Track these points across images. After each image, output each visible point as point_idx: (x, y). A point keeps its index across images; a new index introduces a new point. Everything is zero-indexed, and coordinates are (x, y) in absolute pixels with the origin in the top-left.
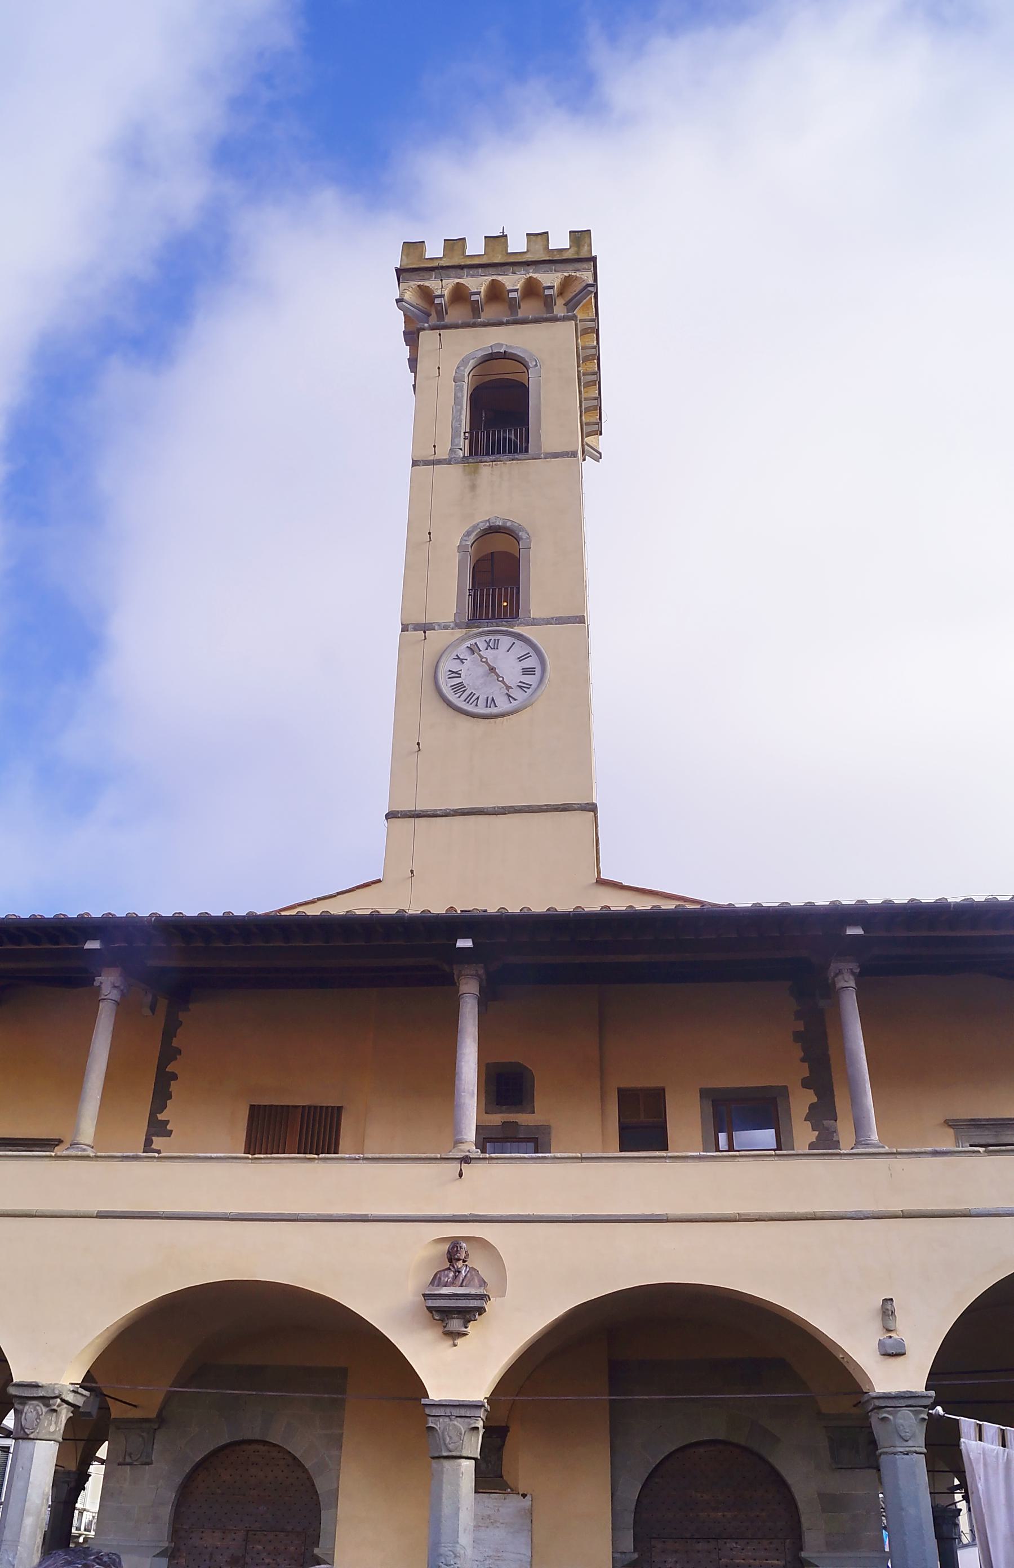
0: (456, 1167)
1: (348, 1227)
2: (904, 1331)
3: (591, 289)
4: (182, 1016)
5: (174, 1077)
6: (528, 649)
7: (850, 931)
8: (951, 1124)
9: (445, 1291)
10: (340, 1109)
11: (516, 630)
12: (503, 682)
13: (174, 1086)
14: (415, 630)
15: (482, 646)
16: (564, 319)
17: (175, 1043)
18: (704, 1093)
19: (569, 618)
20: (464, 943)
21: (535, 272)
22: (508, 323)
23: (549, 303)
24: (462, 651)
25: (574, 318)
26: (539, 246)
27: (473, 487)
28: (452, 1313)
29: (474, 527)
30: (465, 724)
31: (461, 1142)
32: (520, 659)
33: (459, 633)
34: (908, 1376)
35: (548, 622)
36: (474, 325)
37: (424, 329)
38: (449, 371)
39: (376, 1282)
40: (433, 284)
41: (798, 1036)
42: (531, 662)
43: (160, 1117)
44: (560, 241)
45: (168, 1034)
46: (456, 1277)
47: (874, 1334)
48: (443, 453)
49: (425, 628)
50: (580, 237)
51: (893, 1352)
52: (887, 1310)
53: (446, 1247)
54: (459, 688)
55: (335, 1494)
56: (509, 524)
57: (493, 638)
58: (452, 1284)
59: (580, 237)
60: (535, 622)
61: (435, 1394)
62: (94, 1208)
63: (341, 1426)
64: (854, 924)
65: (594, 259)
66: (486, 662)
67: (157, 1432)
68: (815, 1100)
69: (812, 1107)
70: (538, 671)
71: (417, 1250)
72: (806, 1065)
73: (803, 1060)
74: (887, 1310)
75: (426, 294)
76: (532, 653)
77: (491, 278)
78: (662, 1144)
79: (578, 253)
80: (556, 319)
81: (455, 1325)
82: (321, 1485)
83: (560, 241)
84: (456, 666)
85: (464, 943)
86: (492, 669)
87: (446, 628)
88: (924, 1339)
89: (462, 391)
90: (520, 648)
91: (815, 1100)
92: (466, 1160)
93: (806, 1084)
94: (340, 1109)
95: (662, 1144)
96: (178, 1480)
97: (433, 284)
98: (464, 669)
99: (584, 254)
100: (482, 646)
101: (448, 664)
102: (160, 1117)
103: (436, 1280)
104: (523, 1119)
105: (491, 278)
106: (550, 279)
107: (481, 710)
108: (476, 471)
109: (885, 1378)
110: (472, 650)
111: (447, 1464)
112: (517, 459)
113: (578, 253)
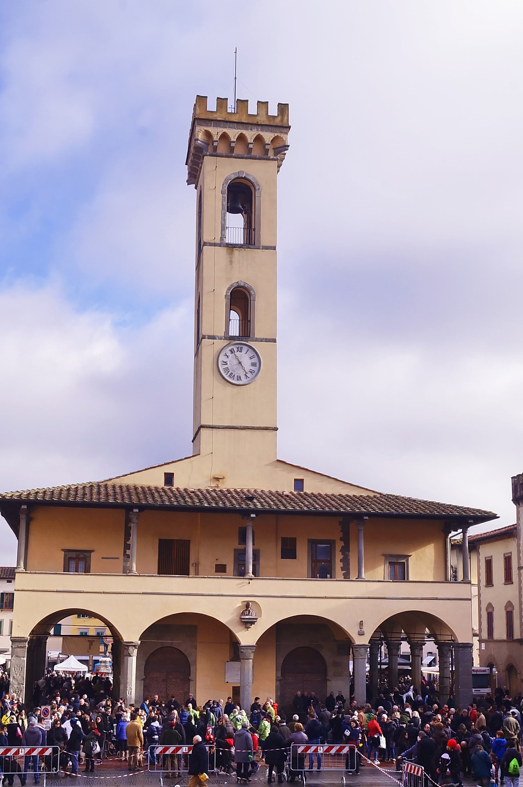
0: (247, 581)
2: (365, 629)
6: (254, 354)
8: (384, 555)
9: (247, 617)
11: (250, 343)
12: (244, 369)
14: (208, 338)
15: (235, 350)
16: (273, 159)
19: (270, 339)
20: (253, 516)
21: (262, 131)
22: (246, 158)
24: (227, 351)
26: (263, 113)
27: (231, 262)
28: (247, 623)
29: (232, 285)
30: (229, 388)
31: (249, 573)
32: (251, 358)
33: (226, 342)
34: (365, 640)
35: (262, 340)
37: (206, 155)
38: (220, 188)
41: (340, 523)
42: (255, 360)
43: (128, 543)
46: (249, 613)
48: (218, 241)
51: (361, 634)
52: (361, 623)
53: (246, 603)
55: (195, 662)
56: (246, 285)
57: (240, 346)
58: (248, 615)
59: (283, 108)
61: (243, 643)
66: (238, 359)
70: (258, 364)
72: (342, 533)
73: (341, 531)
74: (361, 623)
75: (208, 134)
76: (255, 356)
78: (295, 557)
79: (282, 120)
80: (269, 159)
81: (248, 625)
83: (273, 111)
85: (253, 516)
86: (240, 363)
87: (221, 339)
88: (370, 631)
90: (251, 353)
92: (251, 579)
93: (341, 539)
94: (189, 541)
95: (295, 557)
96: (146, 658)
100: (235, 350)
101: (222, 358)
103: (243, 613)
106: (268, 136)
109: (359, 641)
110: (232, 351)
111: (246, 660)
112: (250, 248)
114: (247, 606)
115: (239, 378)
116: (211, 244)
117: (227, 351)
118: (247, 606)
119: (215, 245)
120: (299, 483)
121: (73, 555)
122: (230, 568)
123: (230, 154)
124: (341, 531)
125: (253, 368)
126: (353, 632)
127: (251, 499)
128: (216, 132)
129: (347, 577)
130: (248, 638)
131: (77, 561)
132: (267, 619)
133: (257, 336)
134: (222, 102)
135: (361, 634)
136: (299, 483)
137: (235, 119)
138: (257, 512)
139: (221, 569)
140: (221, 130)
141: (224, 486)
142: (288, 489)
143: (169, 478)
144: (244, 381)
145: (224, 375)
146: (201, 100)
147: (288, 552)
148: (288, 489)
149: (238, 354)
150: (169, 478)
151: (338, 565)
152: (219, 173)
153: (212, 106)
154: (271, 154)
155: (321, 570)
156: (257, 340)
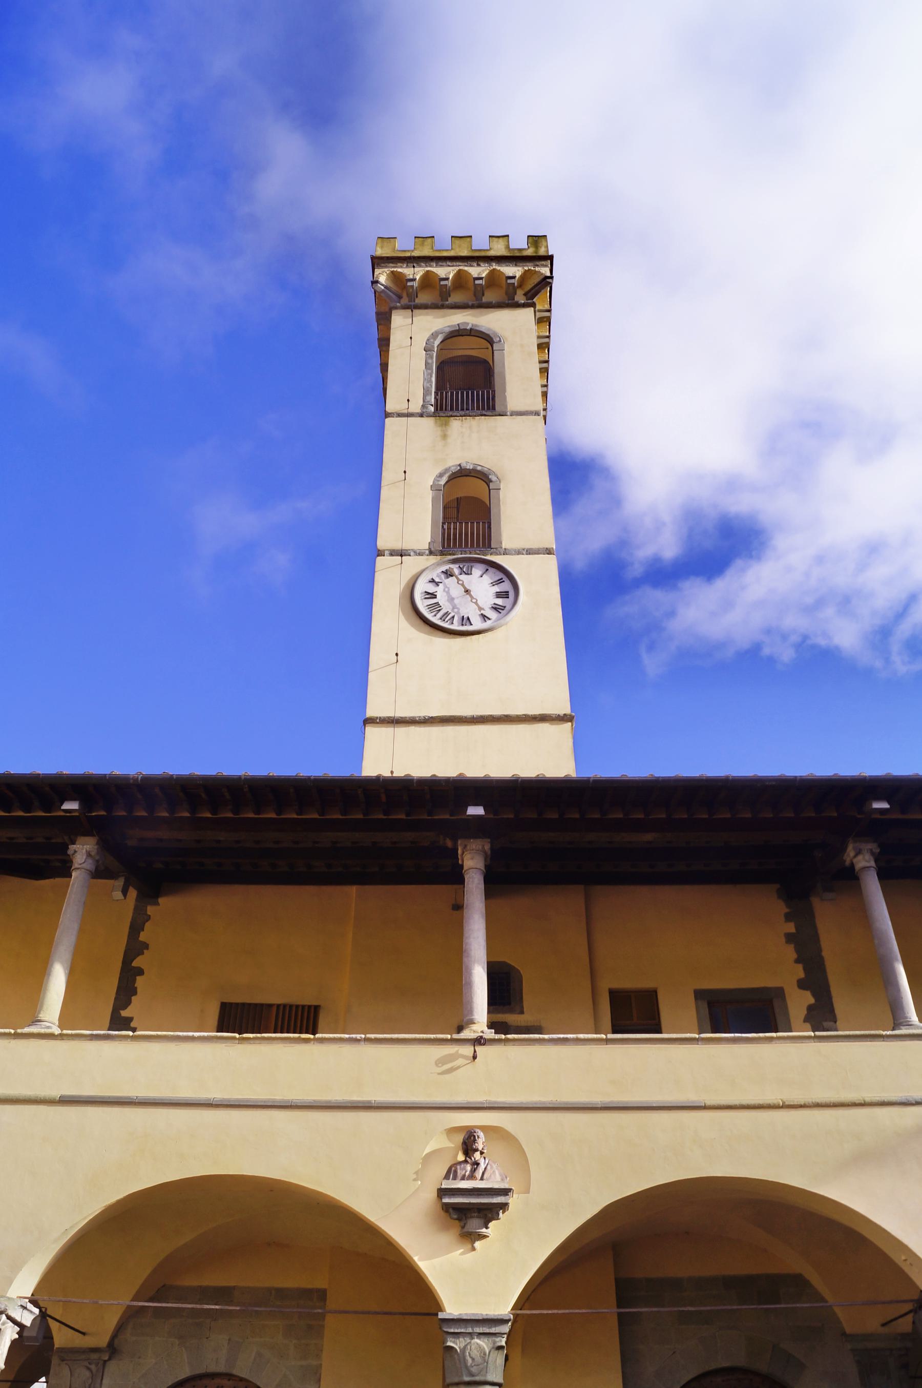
0: (468, 1050)
3: (546, 282)
4: (150, 910)
5: (140, 972)
6: (500, 575)
7: (877, 805)
10: (317, 1008)
11: (488, 557)
12: (476, 603)
13: (140, 981)
14: (391, 555)
15: (456, 571)
16: (524, 306)
17: (143, 937)
18: (699, 995)
19: (539, 549)
22: (472, 307)
24: (436, 574)
25: (533, 305)
27: (445, 436)
28: (468, 1213)
29: (446, 470)
31: (472, 1022)
33: (433, 559)
35: (519, 552)
36: (442, 307)
37: (396, 308)
40: (407, 271)
41: (789, 938)
44: (519, 242)
45: (136, 928)
46: (473, 1171)
50: (536, 240)
53: (460, 1138)
54: (436, 607)
56: (479, 468)
57: (467, 565)
58: (472, 1177)
60: (506, 552)
61: (452, 1308)
62: (56, 1093)
63: (318, 1357)
64: (879, 799)
65: (551, 258)
66: (463, 585)
67: (108, 1363)
68: (812, 1000)
69: (810, 1008)
70: (512, 594)
71: (435, 1138)
73: (797, 961)
76: (505, 578)
77: (458, 268)
80: (517, 306)
81: (473, 1224)
84: (431, 588)
86: (467, 591)
87: (421, 554)
89: (432, 358)
91: (812, 1000)
94: (317, 1008)
97: (407, 271)
98: (439, 591)
99: (542, 252)
100: (456, 571)
101: (422, 586)
102: (124, 1013)
103: (451, 1173)
105: (458, 268)
107: (456, 626)
108: (446, 424)
112: (485, 415)
113: (536, 252)
114: (468, 1147)
115: (466, 620)
116: (400, 415)
118: (468, 1147)
124: (797, 961)
125: (500, 601)
133: (506, 544)
137: (445, 254)
144: (477, 624)
145: (429, 616)
149: (463, 577)
154: (520, 298)
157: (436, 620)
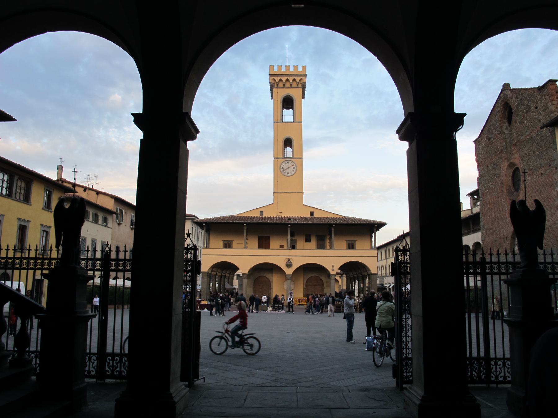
1: (276, 254)
2: (334, 268)
23: (298, 85)
39: (281, 263)
47: (331, 268)
48: (279, 121)
49: (277, 158)
51: (333, 270)
52: (333, 266)
59: (304, 67)
74: (333, 266)
75: (275, 80)
77: (286, 78)
82: (271, 280)
83: (300, 69)
90: (293, 164)
97: (276, 78)
104: (294, 238)
105: (286, 78)
106: (298, 79)
109: (332, 272)
117: (284, 164)
119: (278, 122)
120: (312, 214)
121: (226, 242)
122: (285, 247)
123: (284, 87)
126: (329, 269)
127: (290, 219)
128: (277, 79)
129: (331, 248)
130: (289, 272)
131: (228, 245)
132: (296, 266)
134: (279, 67)
135: (333, 270)
136: (312, 214)
138: (291, 224)
139: (282, 246)
140: (279, 78)
141: (283, 215)
142: (308, 215)
143: (261, 212)
146: (272, 67)
147: (308, 240)
148: (308, 215)
150: (261, 212)
151: (328, 244)
152: (282, 93)
153: (276, 69)
155: (321, 246)
156: (295, 158)
157: (284, 173)
